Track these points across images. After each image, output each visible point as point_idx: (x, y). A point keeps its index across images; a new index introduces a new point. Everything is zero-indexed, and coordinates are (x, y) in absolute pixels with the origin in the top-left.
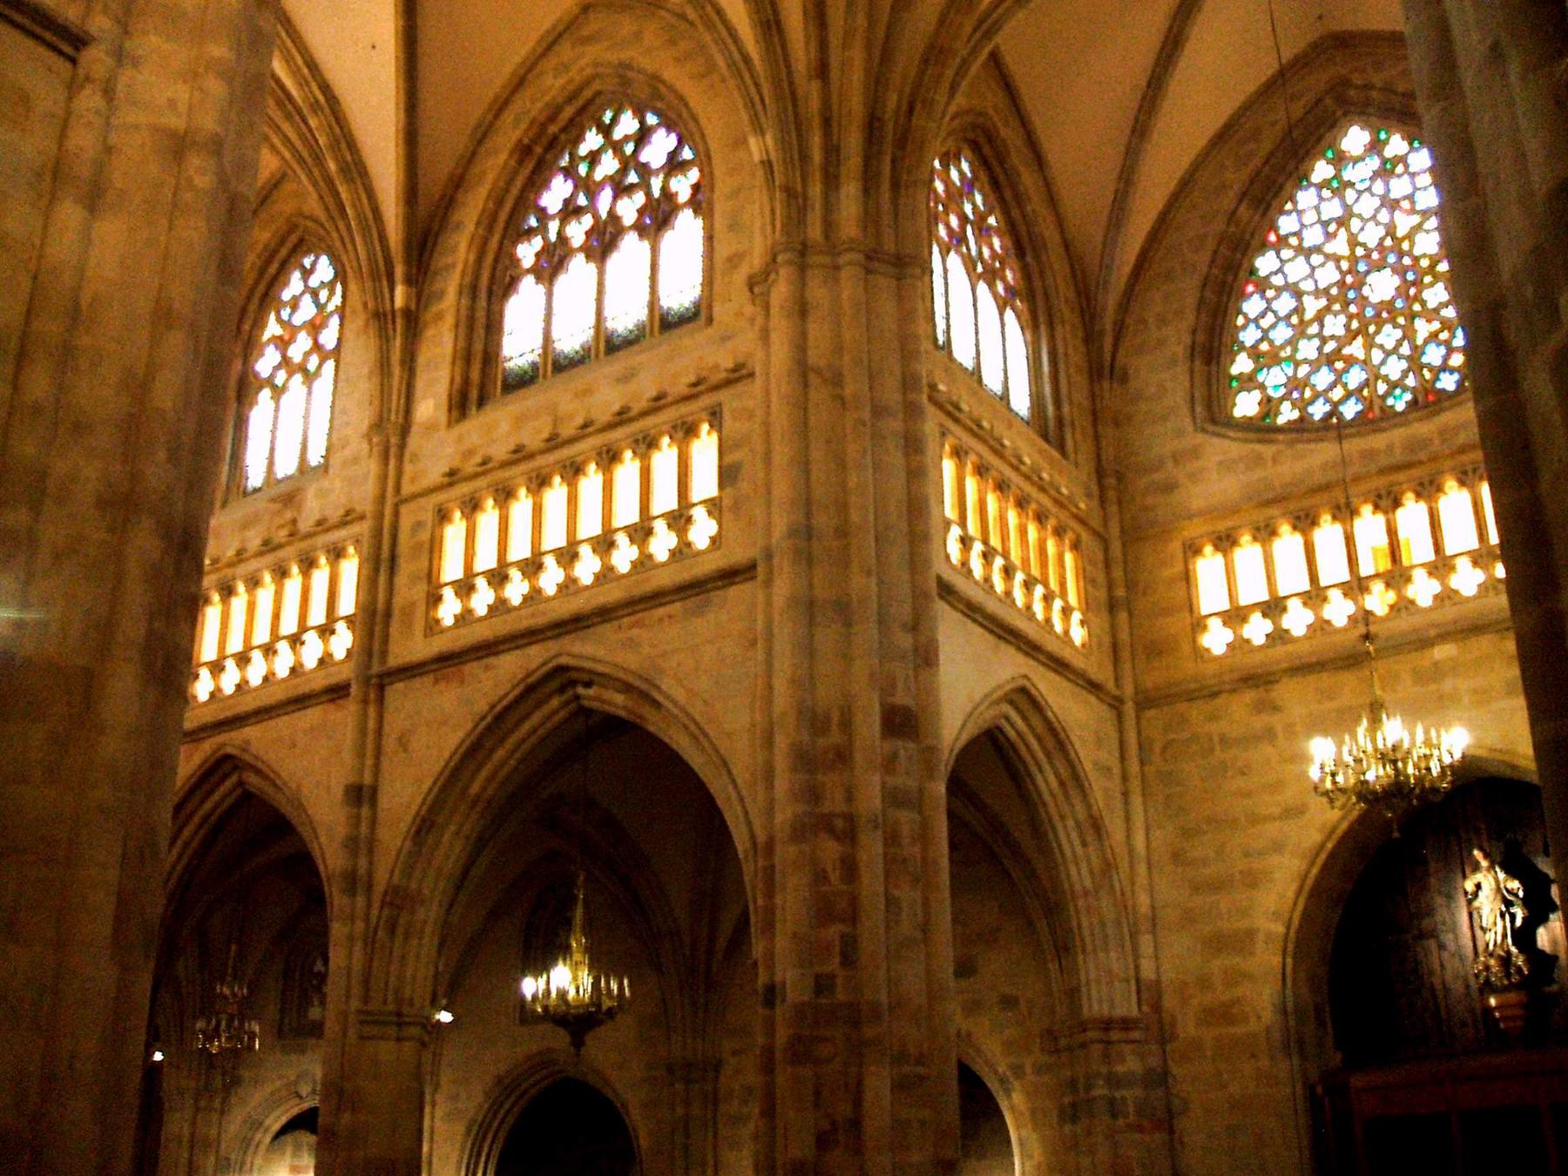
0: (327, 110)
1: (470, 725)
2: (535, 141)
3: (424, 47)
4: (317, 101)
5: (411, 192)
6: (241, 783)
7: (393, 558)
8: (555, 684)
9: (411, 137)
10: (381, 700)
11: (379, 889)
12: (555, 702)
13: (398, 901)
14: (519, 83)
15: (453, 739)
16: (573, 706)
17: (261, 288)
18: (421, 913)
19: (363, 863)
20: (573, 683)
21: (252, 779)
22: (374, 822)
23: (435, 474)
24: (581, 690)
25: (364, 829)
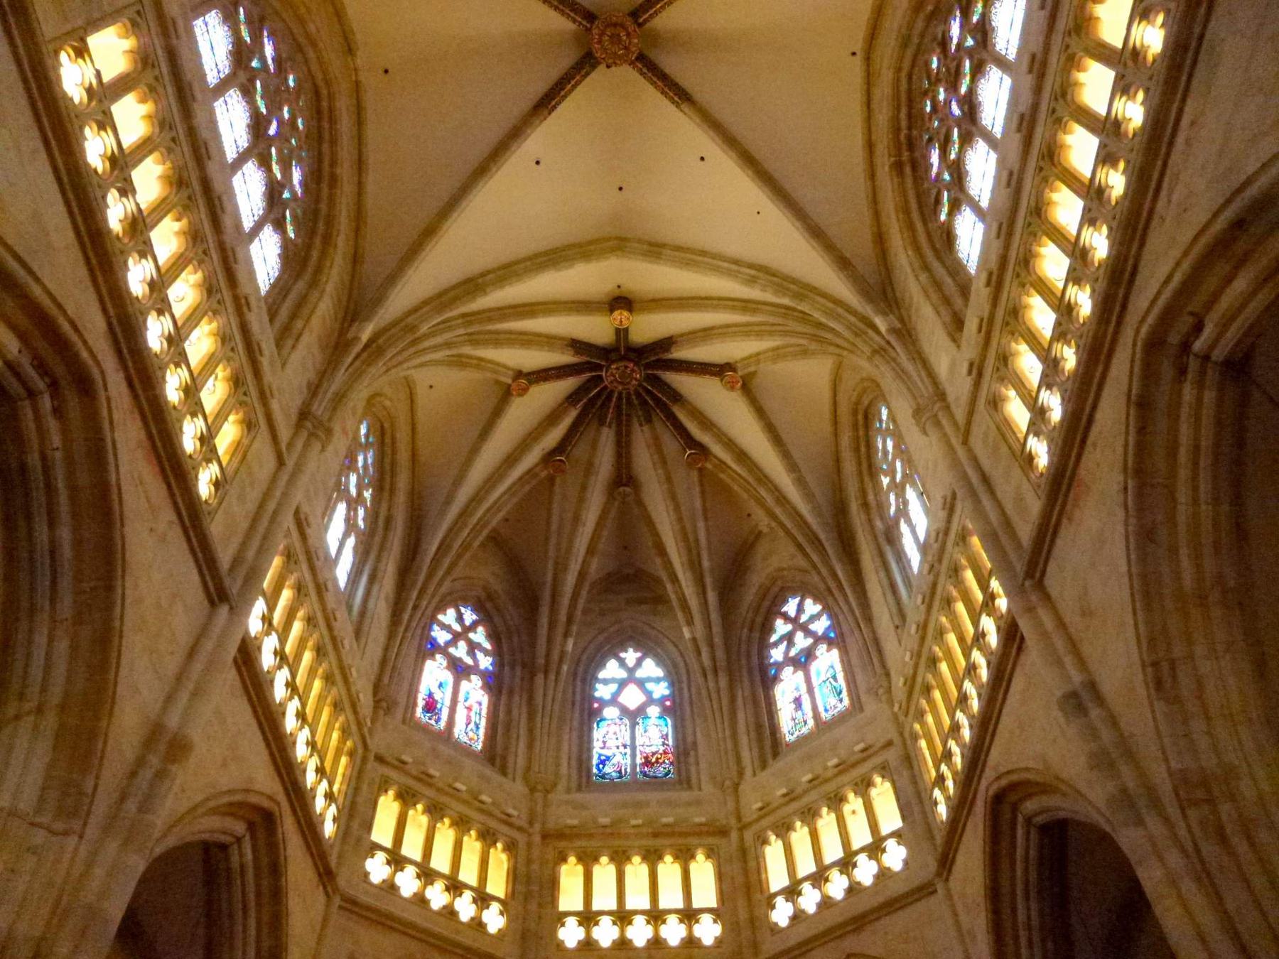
0: (761, 275)
1: (1120, 514)
2: (899, 155)
3: (771, 165)
4: (750, 275)
5: (843, 263)
6: (1028, 821)
7: (985, 479)
8: (1167, 370)
9: (816, 232)
10: (1047, 597)
11: (1166, 789)
12: (1188, 393)
13: (1200, 794)
14: (870, 146)
15: (1117, 552)
16: (1212, 375)
17: (865, 465)
18: (1246, 789)
19: (1126, 771)
20: (1185, 347)
21: (1030, 806)
22: (1113, 722)
23: (966, 384)
24: (1198, 345)
25: (1106, 735)
